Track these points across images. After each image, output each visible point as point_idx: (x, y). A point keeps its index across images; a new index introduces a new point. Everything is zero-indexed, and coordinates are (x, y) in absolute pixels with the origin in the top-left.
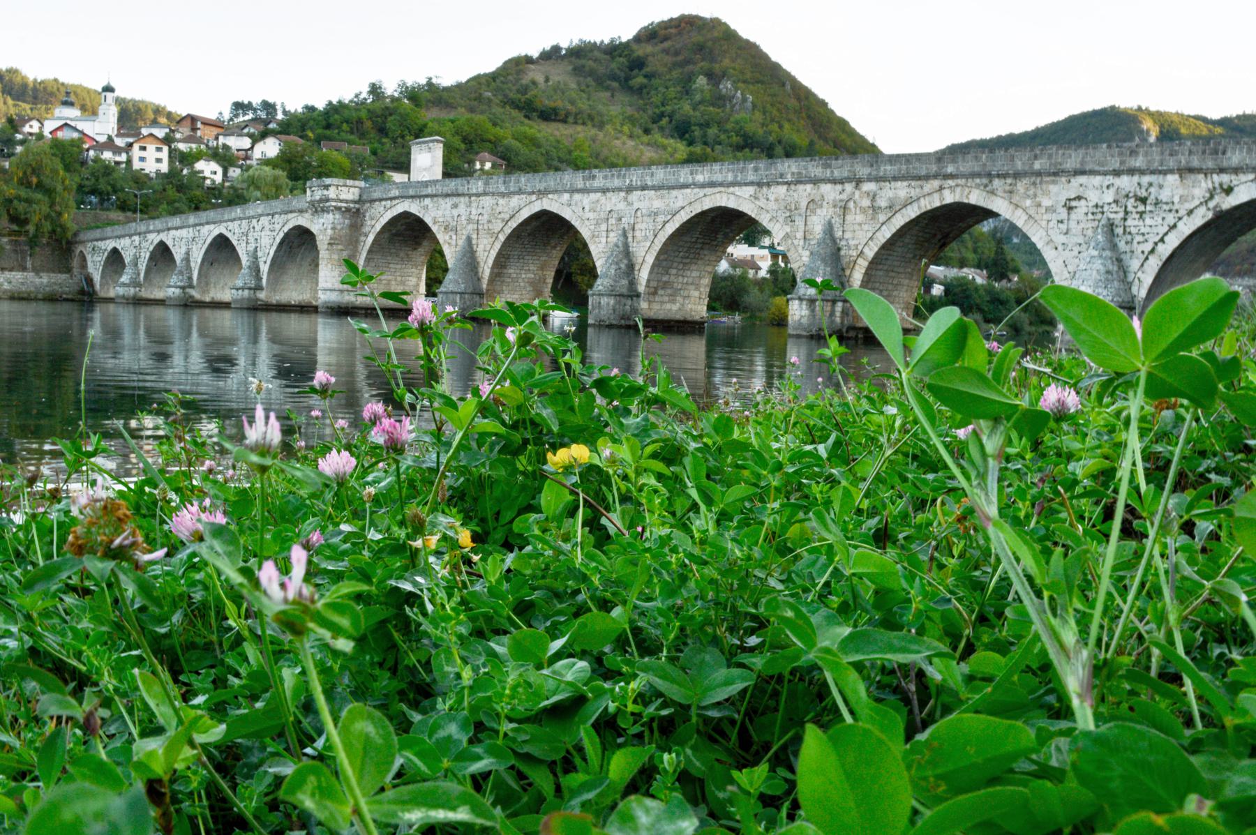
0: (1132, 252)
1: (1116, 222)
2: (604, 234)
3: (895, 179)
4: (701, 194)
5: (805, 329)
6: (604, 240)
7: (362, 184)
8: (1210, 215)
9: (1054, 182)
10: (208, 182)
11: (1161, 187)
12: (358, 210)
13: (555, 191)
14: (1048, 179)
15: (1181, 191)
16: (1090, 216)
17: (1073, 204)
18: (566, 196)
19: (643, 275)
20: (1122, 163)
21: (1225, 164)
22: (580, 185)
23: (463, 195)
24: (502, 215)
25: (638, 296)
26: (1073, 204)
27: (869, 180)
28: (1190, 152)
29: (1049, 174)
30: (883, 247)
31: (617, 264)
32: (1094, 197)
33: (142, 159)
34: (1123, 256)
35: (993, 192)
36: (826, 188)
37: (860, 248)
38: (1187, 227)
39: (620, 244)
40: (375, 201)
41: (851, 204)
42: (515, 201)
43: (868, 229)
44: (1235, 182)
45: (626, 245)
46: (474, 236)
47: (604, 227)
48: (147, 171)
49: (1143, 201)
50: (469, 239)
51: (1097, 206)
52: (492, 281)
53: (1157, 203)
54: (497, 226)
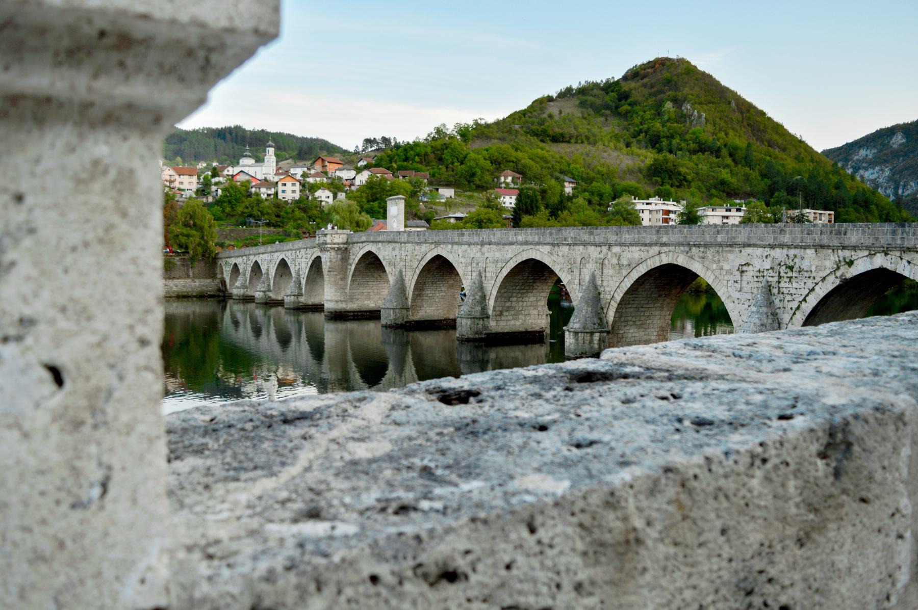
1: (773, 284)
2: (470, 273)
3: (631, 245)
4: (521, 250)
5: (572, 353)
6: (470, 278)
7: (348, 231)
8: (838, 282)
9: (731, 252)
10: (323, 203)
11: (802, 258)
12: (346, 248)
14: (727, 249)
15: (816, 263)
16: (756, 279)
17: (745, 268)
18: (450, 246)
19: (491, 303)
20: (775, 239)
21: (846, 243)
22: (457, 240)
24: (417, 257)
25: (488, 317)
26: (745, 268)
27: (616, 245)
28: (821, 233)
29: (728, 246)
30: (627, 293)
31: (474, 295)
32: (757, 264)
33: (284, 191)
34: (778, 311)
35: (692, 257)
36: (591, 249)
37: (612, 293)
38: (822, 291)
39: (477, 282)
40: (354, 243)
41: (606, 262)
42: (424, 248)
43: (617, 279)
44: (854, 257)
45: (481, 283)
46: (404, 270)
48: (286, 199)
49: (791, 268)
50: (401, 272)
51: (759, 271)
52: (414, 300)
54: (415, 264)
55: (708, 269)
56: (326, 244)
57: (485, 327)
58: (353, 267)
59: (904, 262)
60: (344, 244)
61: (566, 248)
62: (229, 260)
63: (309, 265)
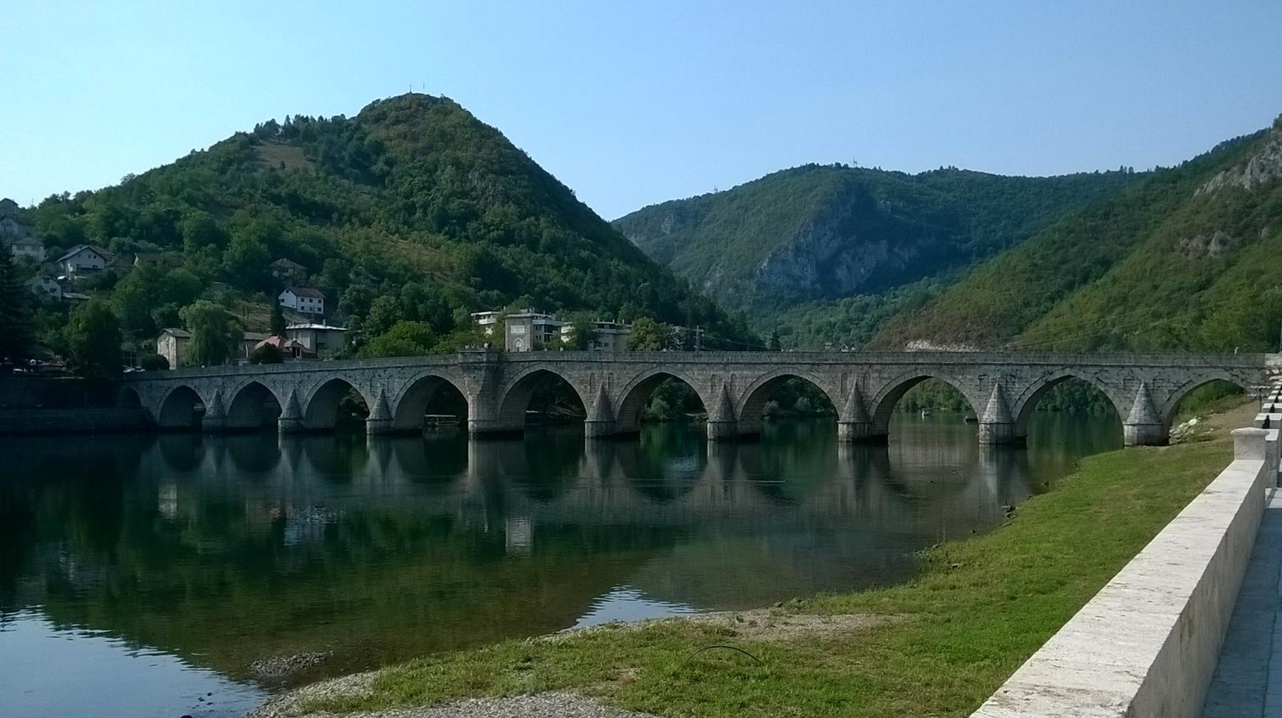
0: (1010, 399)
3: (891, 364)
6: (710, 391)
8: (1044, 384)
9: (973, 368)
13: (670, 363)
17: (982, 377)
18: (680, 365)
19: (739, 410)
21: (1049, 363)
25: (737, 422)
26: (982, 377)
27: (877, 364)
28: (1034, 356)
35: (943, 372)
36: (854, 366)
41: (867, 375)
49: (1014, 376)
50: (603, 388)
56: (483, 362)
57: (736, 429)
58: (510, 386)
59: (1082, 372)
62: (166, 384)
63: (409, 386)
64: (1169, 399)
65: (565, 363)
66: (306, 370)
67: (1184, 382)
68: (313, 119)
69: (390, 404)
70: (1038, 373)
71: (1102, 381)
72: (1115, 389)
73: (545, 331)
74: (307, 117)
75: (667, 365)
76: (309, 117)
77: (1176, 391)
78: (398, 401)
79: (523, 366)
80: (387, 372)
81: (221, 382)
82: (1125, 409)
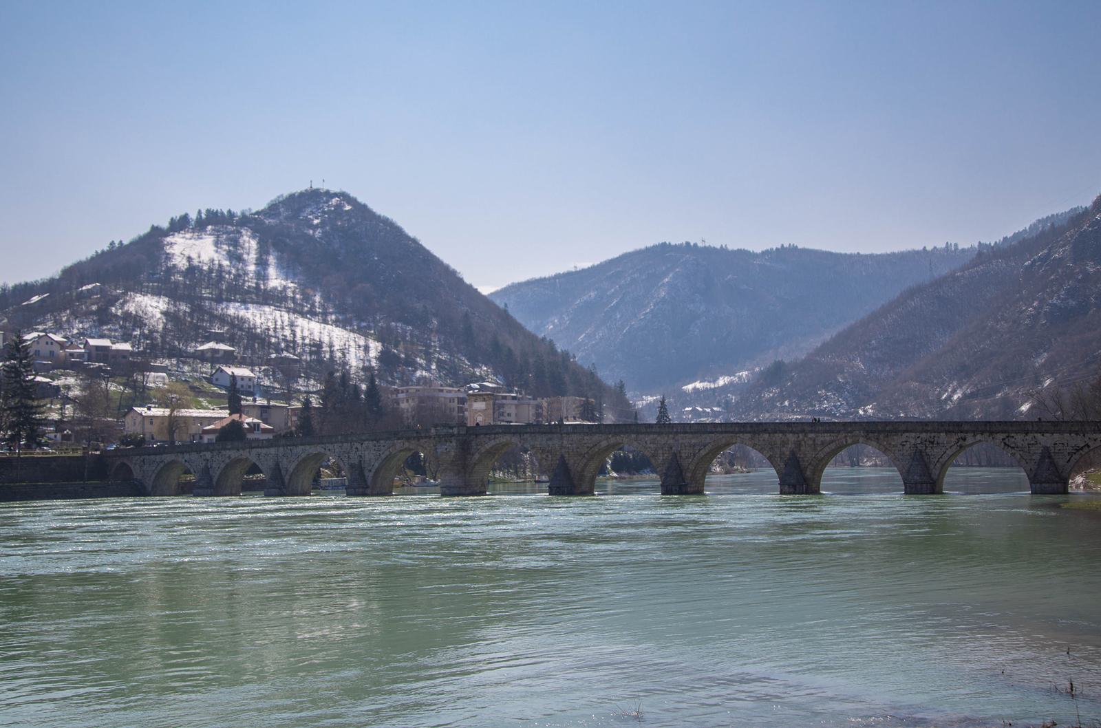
6: (661, 458)
9: (895, 435)
12: (466, 440)
18: (633, 436)
19: (689, 475)
20: (923, 428)
23: (557, 433)
24: (588, 445)
32: (913, 441)
36: (790, 436)
41: (803, 443)
42: (596, 437)
46: (567, 456)
47: (660, 452)
49: (932, 443)
53: (938, 443)
55: (880, 444)
60: (464, 435)
61: (766, 436)
63: (383, 456)
64: (1069, 461)
65: (528, 435)
66: (288, 443)
67: (1082, 445)
68: (222, 213)
69: (366, 473)
70: (952, 440)
71: (1009, 446)
72: (1021, 453)
73: (458, 404)
74: (217, 211)
75: (622, 436)
76: (219, 210)
77: (1075, 453)
78: (373, 471)
79: (489, 438)
80: (363, 445)
81: (210, 456)
82: (1031, 469)
